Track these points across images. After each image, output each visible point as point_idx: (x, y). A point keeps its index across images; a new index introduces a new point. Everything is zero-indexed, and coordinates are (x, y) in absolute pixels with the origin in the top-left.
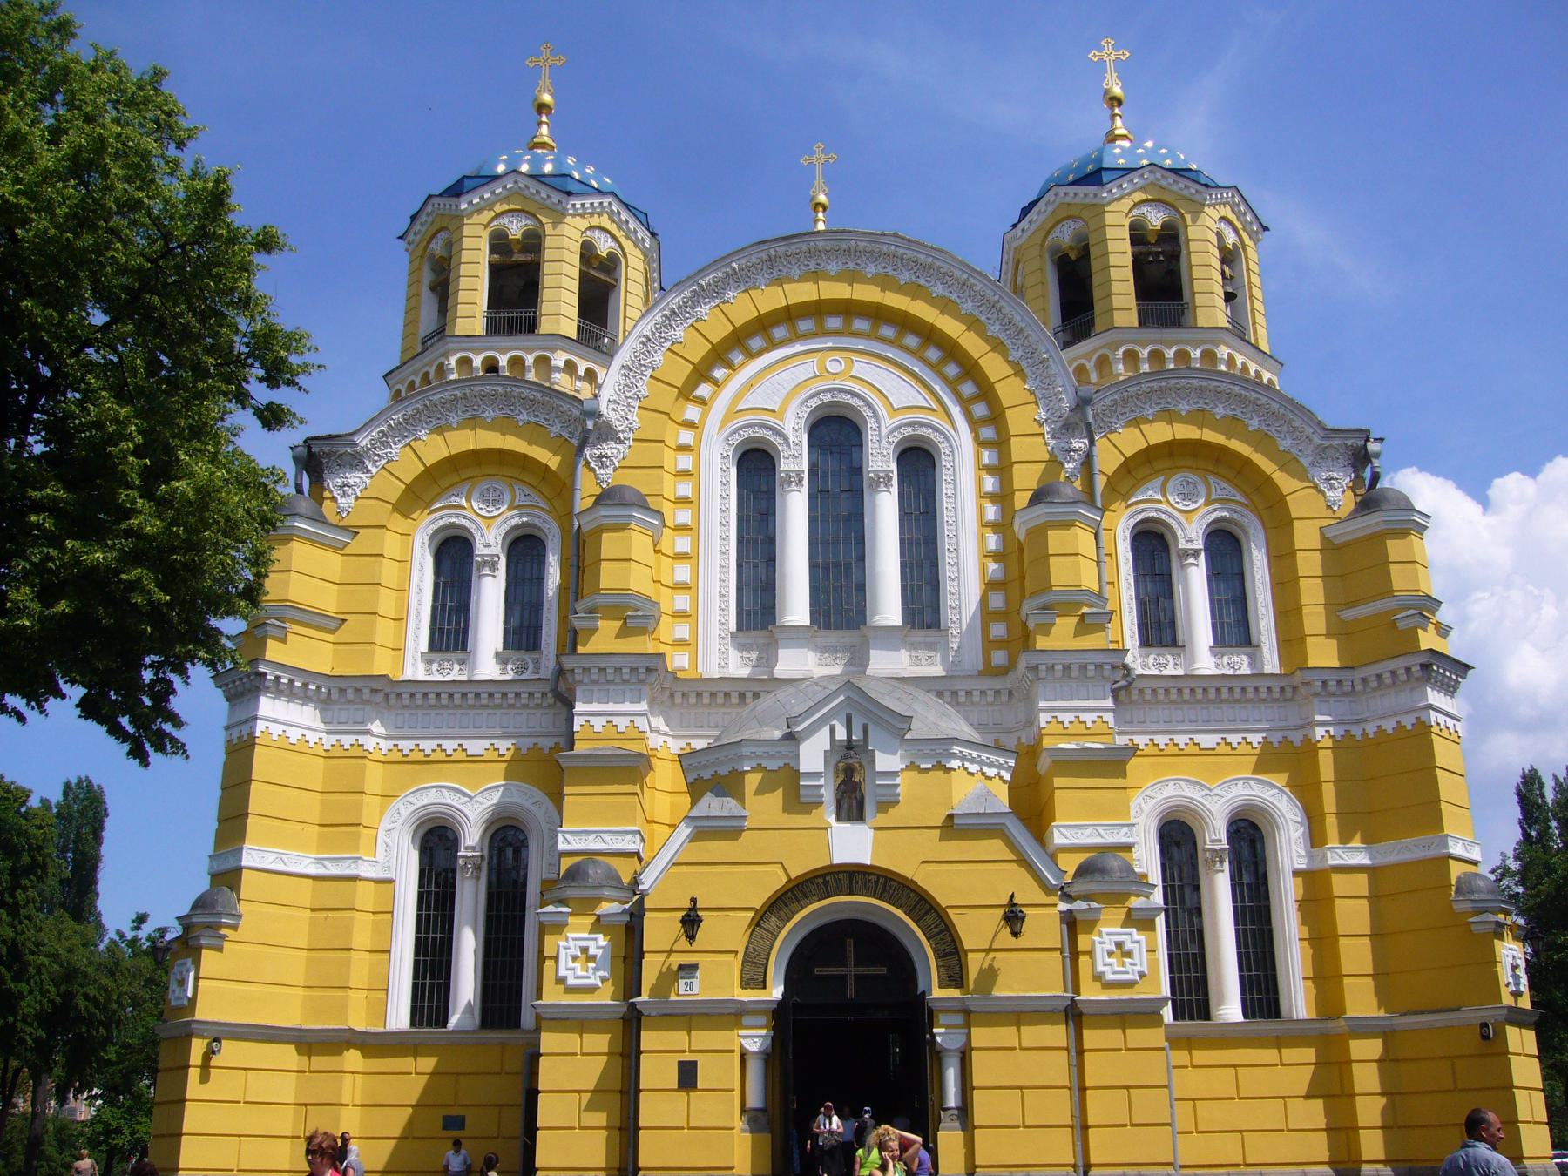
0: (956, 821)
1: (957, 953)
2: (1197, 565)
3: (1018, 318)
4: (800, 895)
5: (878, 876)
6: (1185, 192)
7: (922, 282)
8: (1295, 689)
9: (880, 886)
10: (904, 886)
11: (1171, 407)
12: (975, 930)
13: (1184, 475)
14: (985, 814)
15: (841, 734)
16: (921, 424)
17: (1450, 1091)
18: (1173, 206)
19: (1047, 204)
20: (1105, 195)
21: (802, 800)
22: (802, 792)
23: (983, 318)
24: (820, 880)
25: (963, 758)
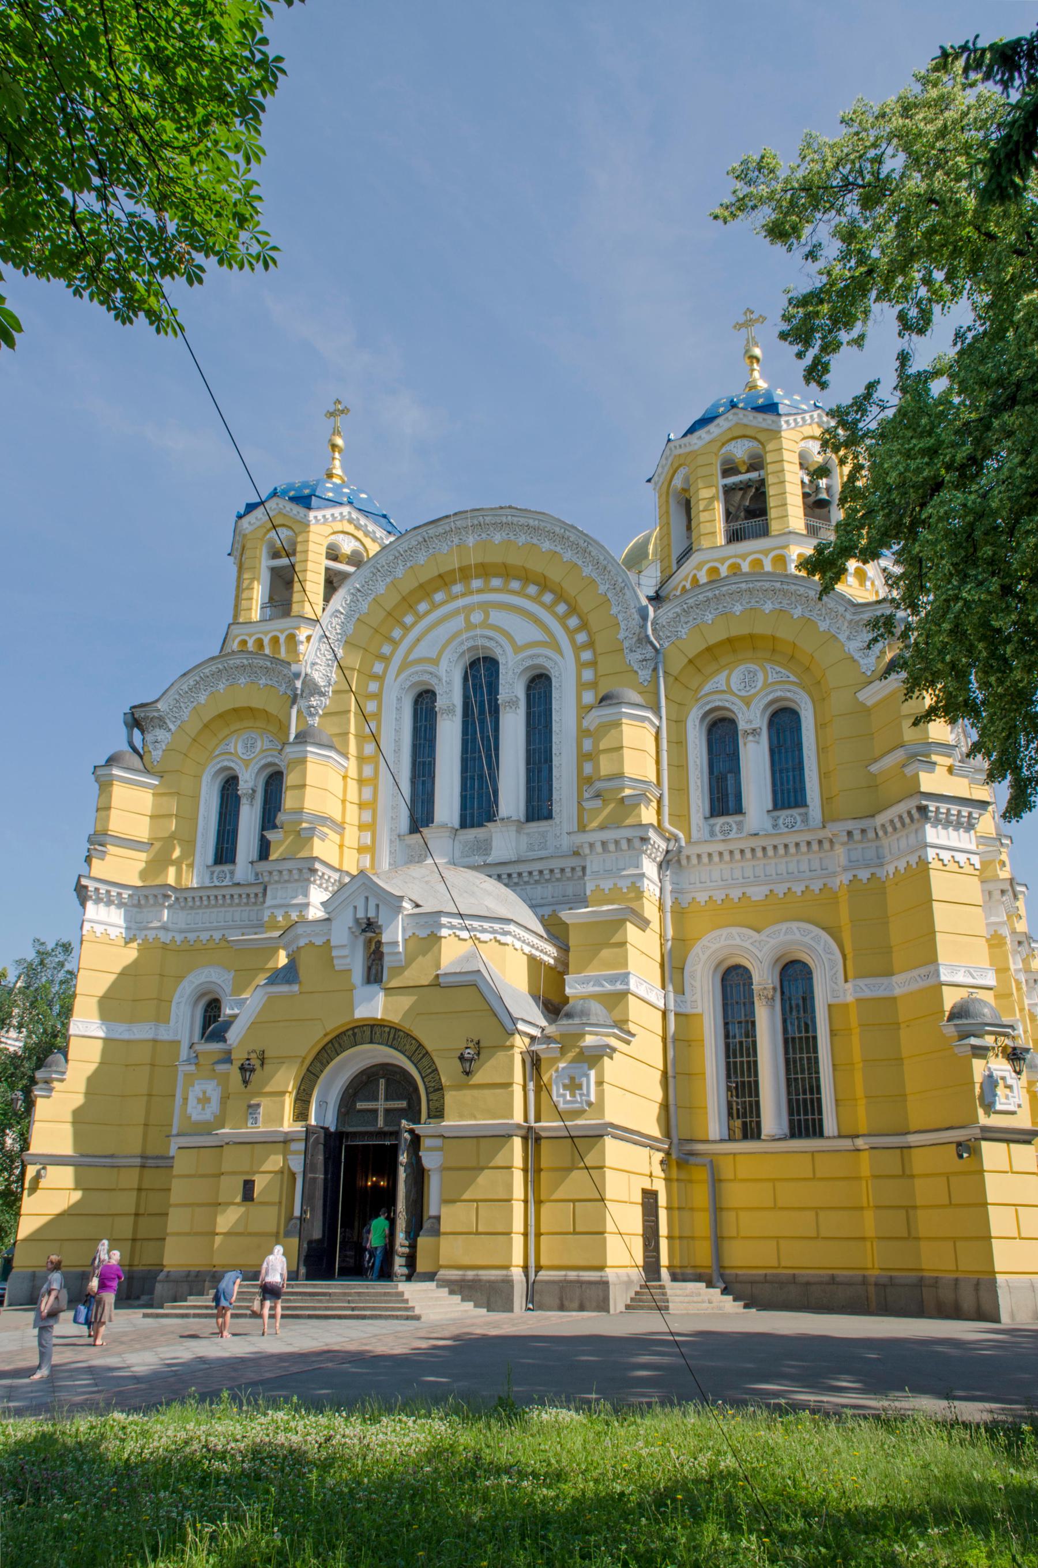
0: (441, 980)
1: (442, 1089)
2: (758, 743)
3: (602, 558)
4: (336, 1045)
5: (391, 1028)
6: (764, 425)
7: (535, 541)
8: (831, 842)
9: (392, 1036)
10: (408, 1035)
11: (728, 610)
12: (448, 1070)
13: (748, 665)
14: (460, 973)
15: (361, 914)
16: (538, 656)
17: (943, 1206)
18: (755, 439)
19: (667, 459)
20: (695, 441)
21: (337, 968)
22: (336, 962)
23: (580, 563)
24: (350, 1033)
25: (452, 927)
